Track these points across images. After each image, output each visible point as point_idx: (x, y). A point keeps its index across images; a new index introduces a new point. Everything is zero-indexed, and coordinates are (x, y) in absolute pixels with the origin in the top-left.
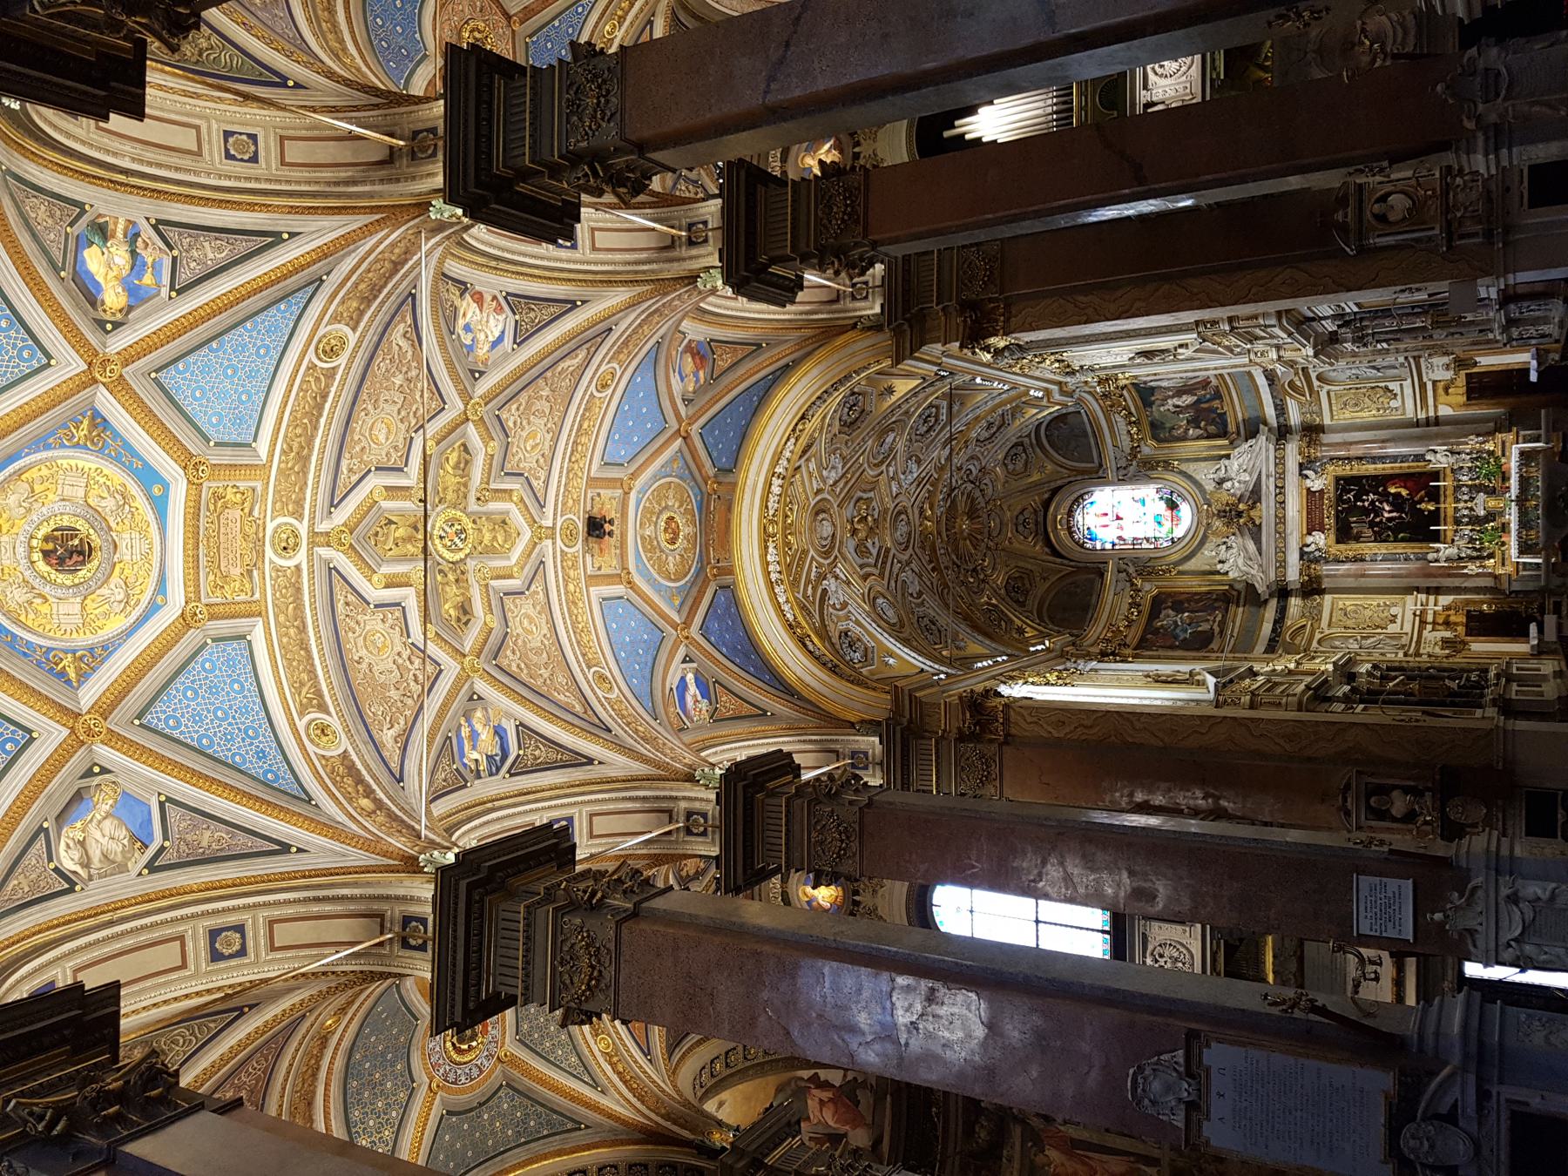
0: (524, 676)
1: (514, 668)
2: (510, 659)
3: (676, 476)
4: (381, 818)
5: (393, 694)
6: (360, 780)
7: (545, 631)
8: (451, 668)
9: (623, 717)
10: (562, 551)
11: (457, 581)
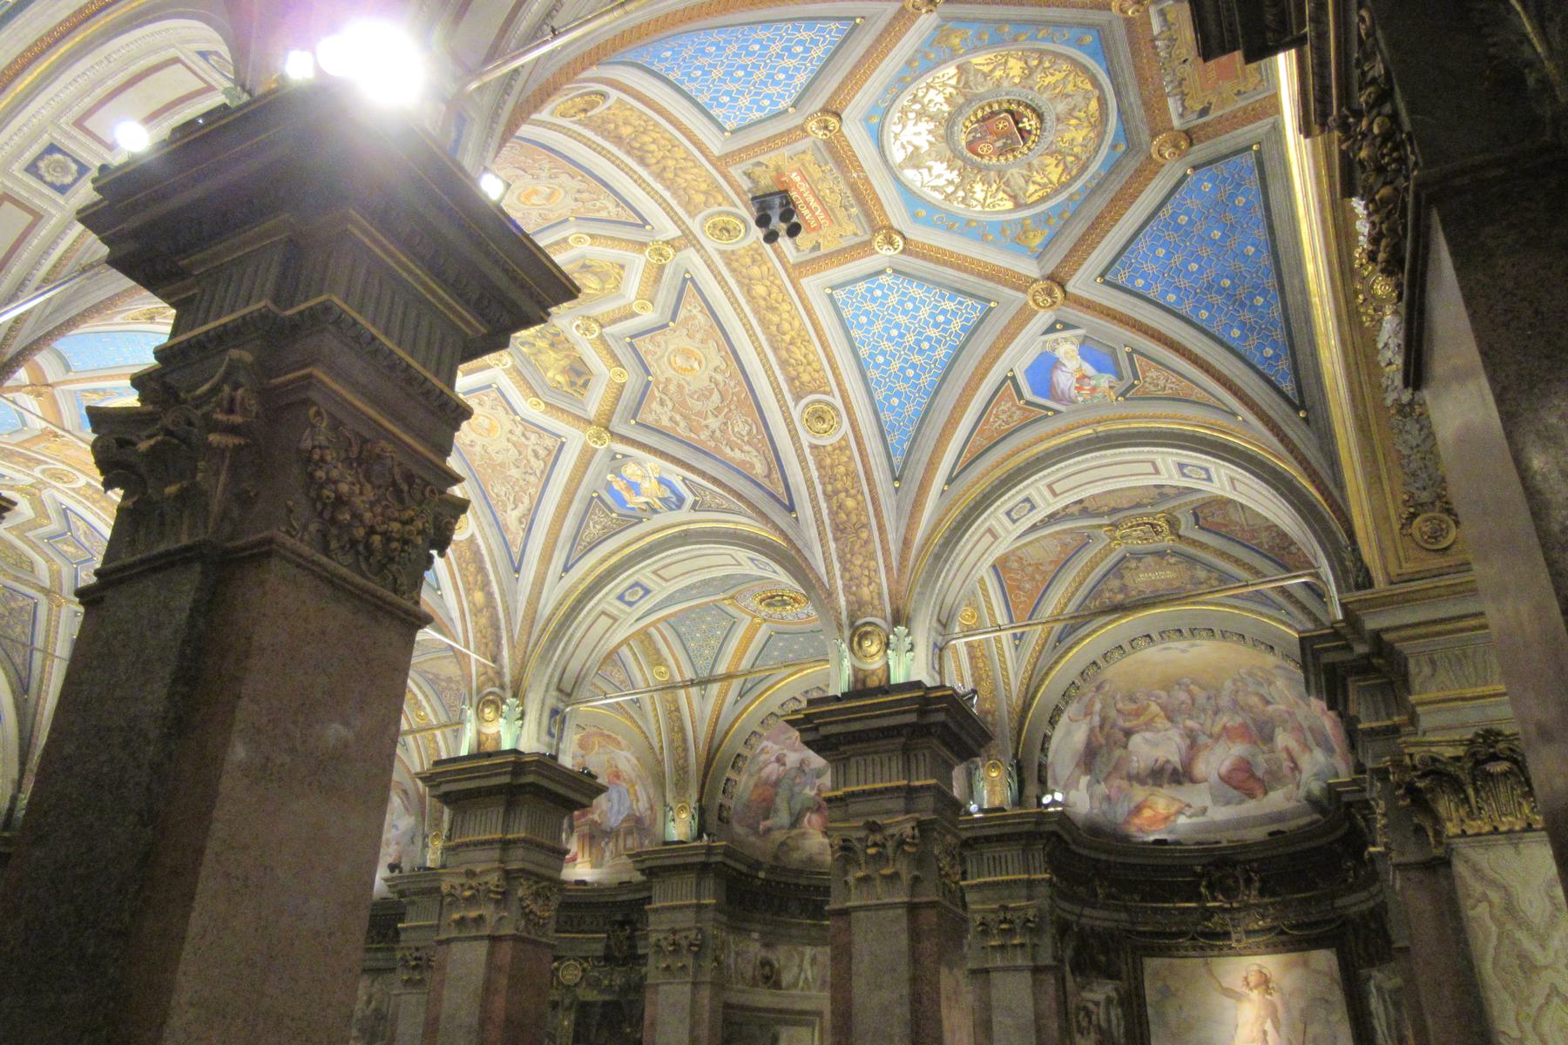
0: (682, 430)
1: (665, 422)
2: (658, 413)
3: (975, 50)
4: (483, 621)
5: (514, 473)
6: (481, 569)
7: (717, 361)
8: (576, 439)
9: (833, 478)
10: (722, 253)
11: (552, 345)
